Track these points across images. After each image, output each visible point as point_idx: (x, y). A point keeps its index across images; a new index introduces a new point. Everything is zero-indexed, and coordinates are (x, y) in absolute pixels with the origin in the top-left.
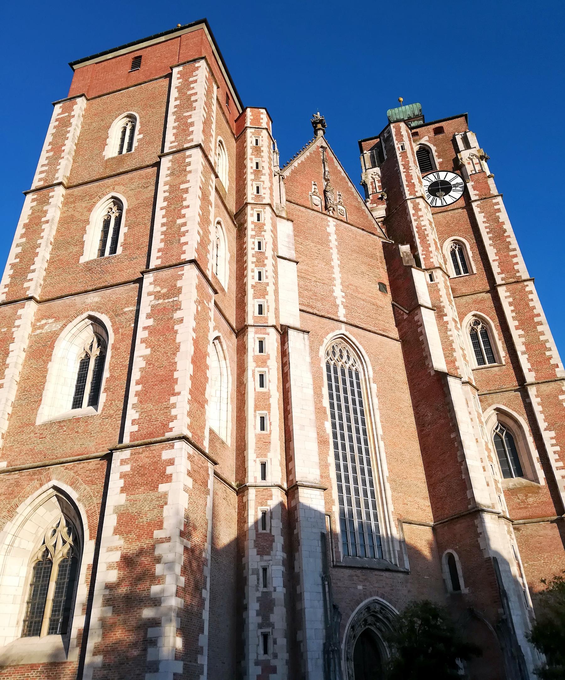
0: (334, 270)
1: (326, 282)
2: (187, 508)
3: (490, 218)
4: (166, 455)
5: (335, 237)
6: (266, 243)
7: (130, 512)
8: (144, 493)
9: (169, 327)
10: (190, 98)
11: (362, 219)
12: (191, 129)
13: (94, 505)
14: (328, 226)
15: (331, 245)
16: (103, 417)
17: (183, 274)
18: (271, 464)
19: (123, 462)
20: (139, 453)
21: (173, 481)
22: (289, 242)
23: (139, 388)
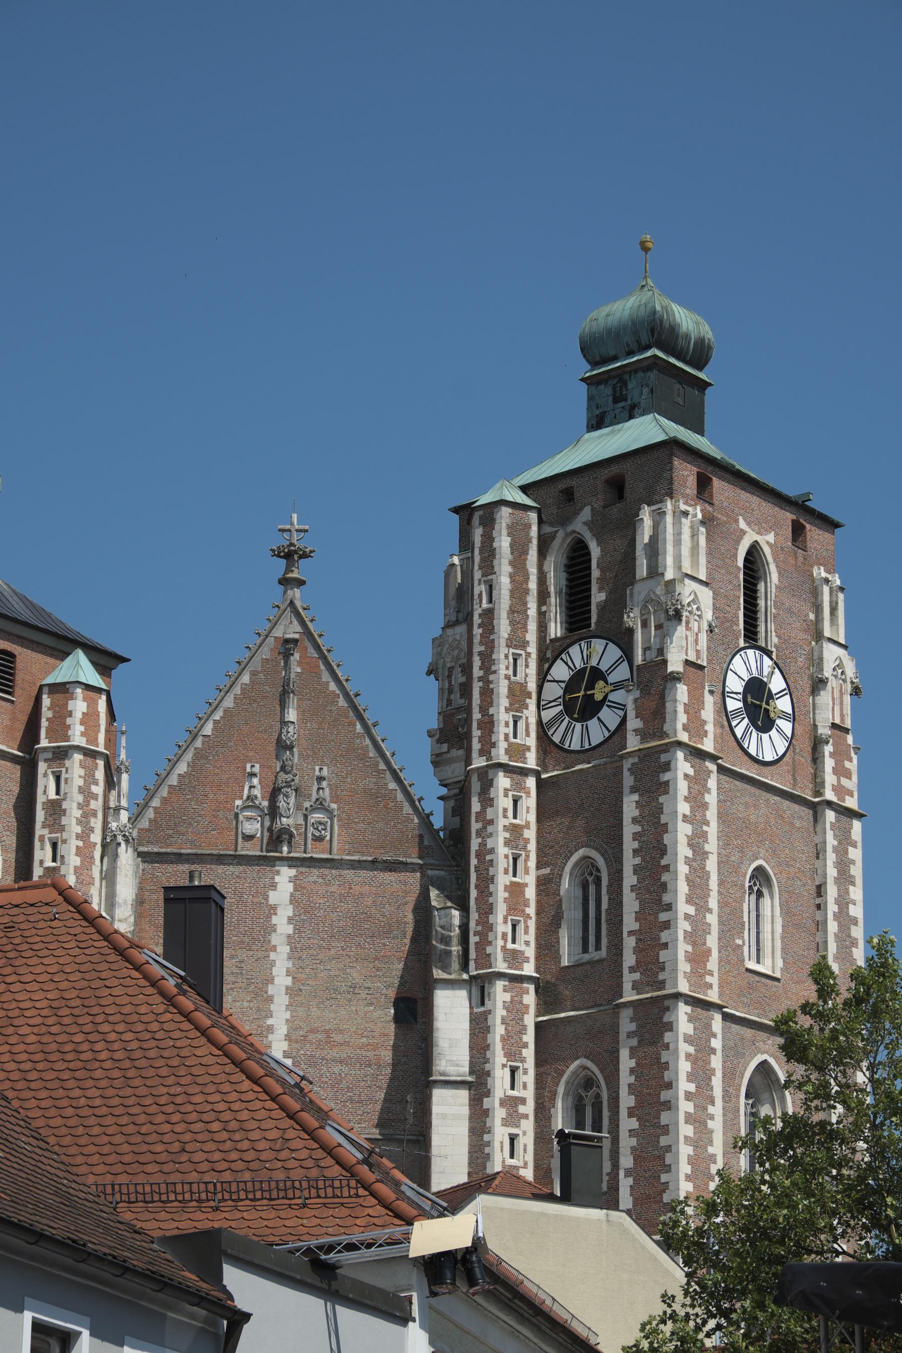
15: (275, 939)
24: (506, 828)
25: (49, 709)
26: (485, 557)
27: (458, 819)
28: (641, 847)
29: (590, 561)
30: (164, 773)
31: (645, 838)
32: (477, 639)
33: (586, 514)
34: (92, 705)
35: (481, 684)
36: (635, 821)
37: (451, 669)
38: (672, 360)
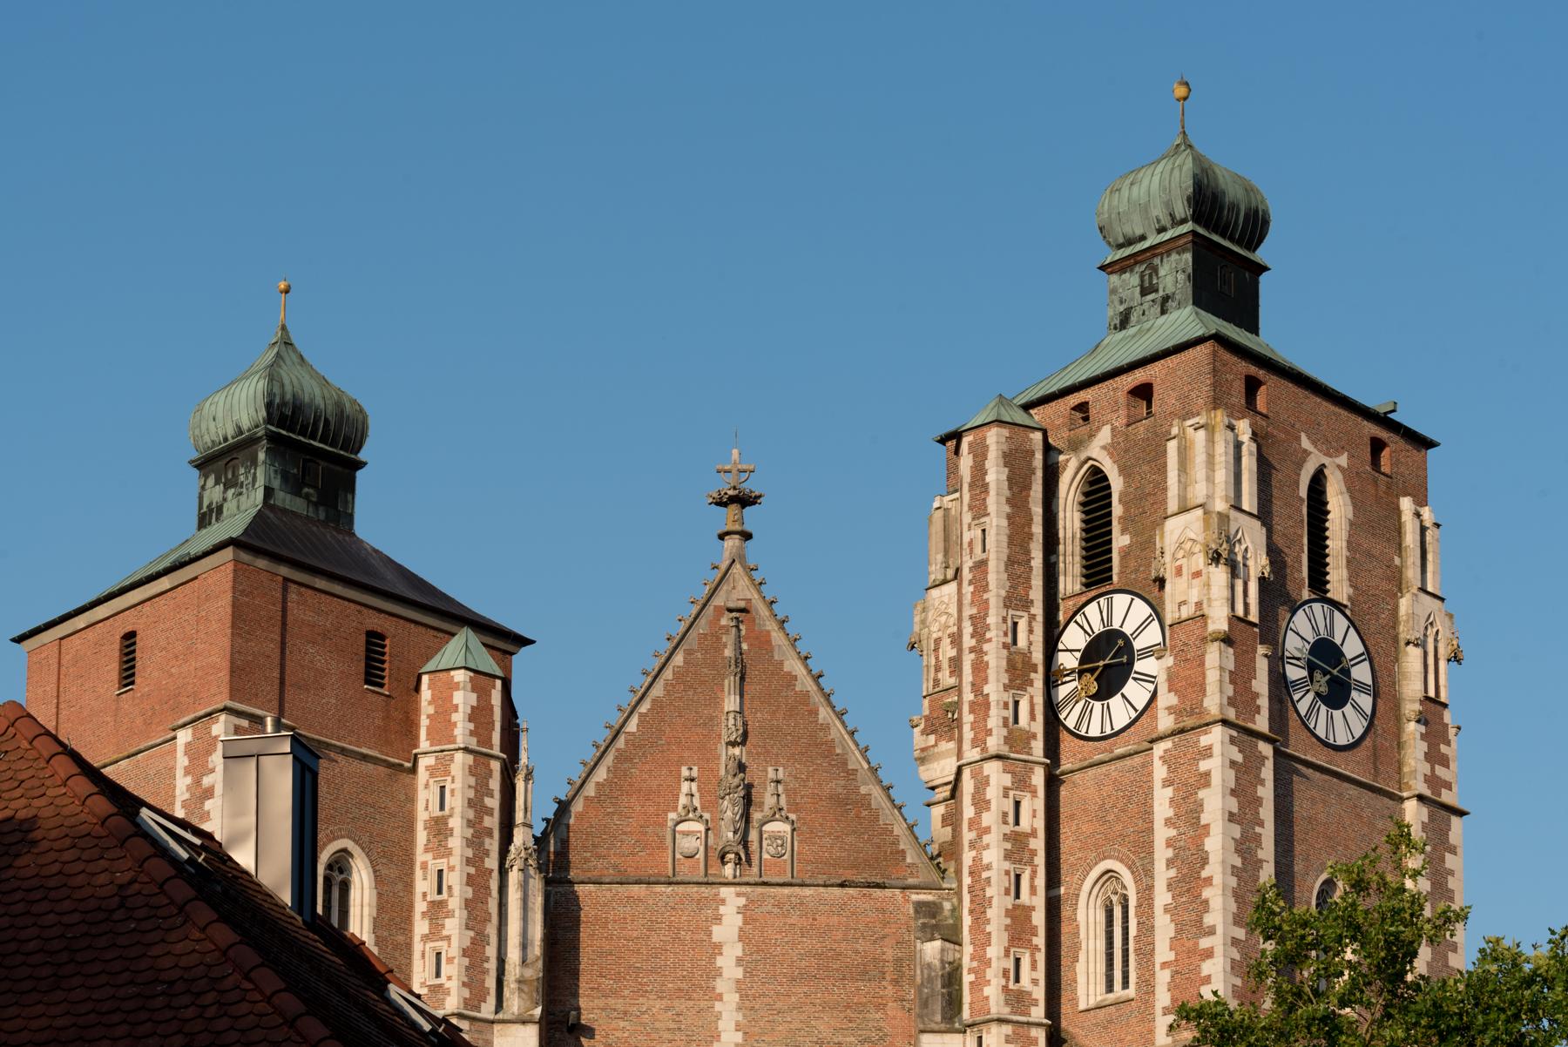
3: (1183, 810)
11: (851, 839)
15: (721, 986)
24: (1006, 837)
25: (430, 703)
26: (976, 495)
27: (949, 829)
28: (1176, 856)
29: (1110, 495)
30: (579, 782)
31: (1182, 843)
32: (967, 599)
33: (1105, 435)
34: (483, 694)
35: (973, 656)
36: (1168, 822)
37: (938, 641)
38: (1216, 238)
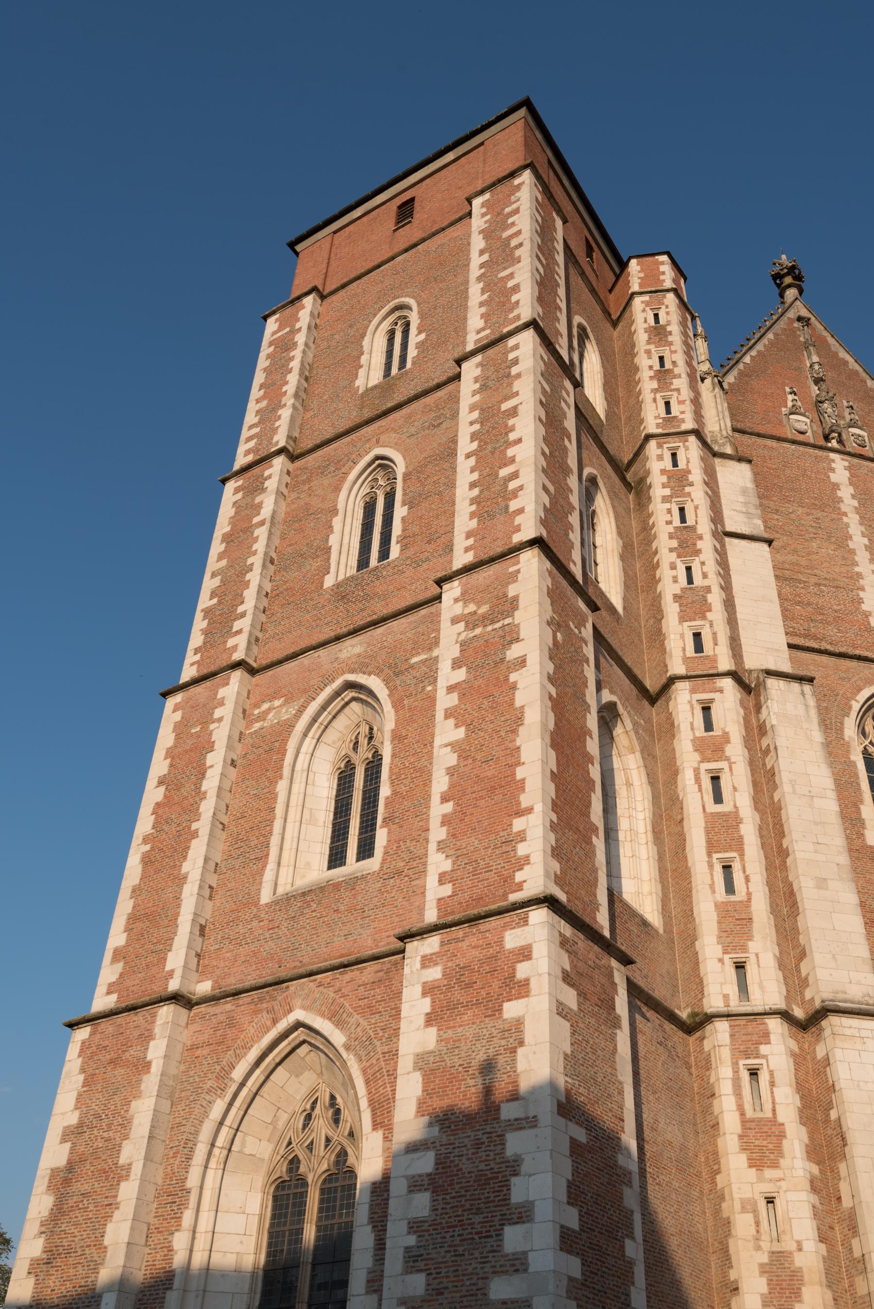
0: (857, 559)
1: (842, 584)
2: (569, 1052)
4: (513, 939)
5: (851, 490)
6: (696, 508)
7: (449, 1065)
8: (473, 1023)
9: (498, 678)
10: (509, 244)
12: (514, 298)
13: (376, 1057)
14: (833, 470)
15: (844, 508)
16: (385, 877)
17: (518, 571)
18: (759, 966)
19: (427, 961)
20: (457, 940)
21: (533, 993)
22: (746, 504)
23: (449, 807)
